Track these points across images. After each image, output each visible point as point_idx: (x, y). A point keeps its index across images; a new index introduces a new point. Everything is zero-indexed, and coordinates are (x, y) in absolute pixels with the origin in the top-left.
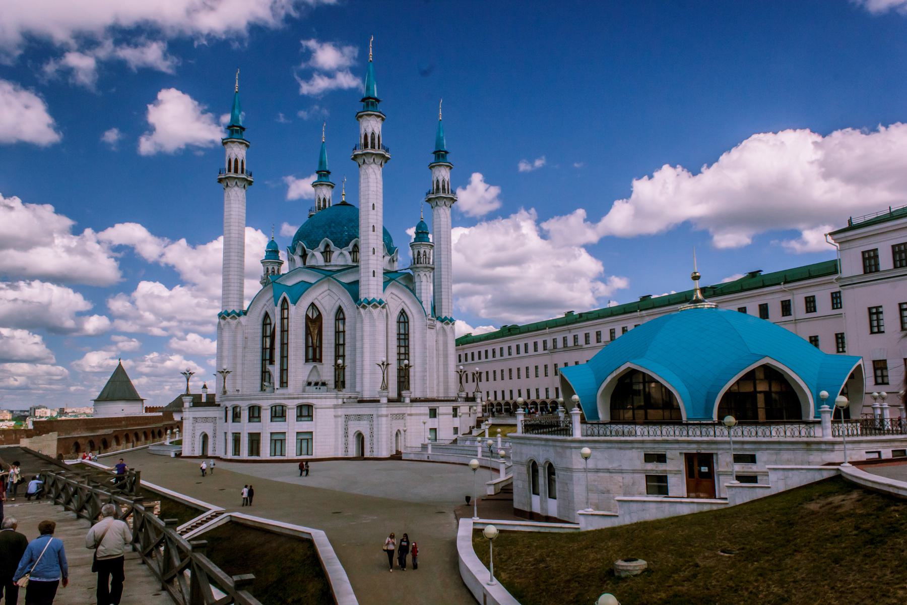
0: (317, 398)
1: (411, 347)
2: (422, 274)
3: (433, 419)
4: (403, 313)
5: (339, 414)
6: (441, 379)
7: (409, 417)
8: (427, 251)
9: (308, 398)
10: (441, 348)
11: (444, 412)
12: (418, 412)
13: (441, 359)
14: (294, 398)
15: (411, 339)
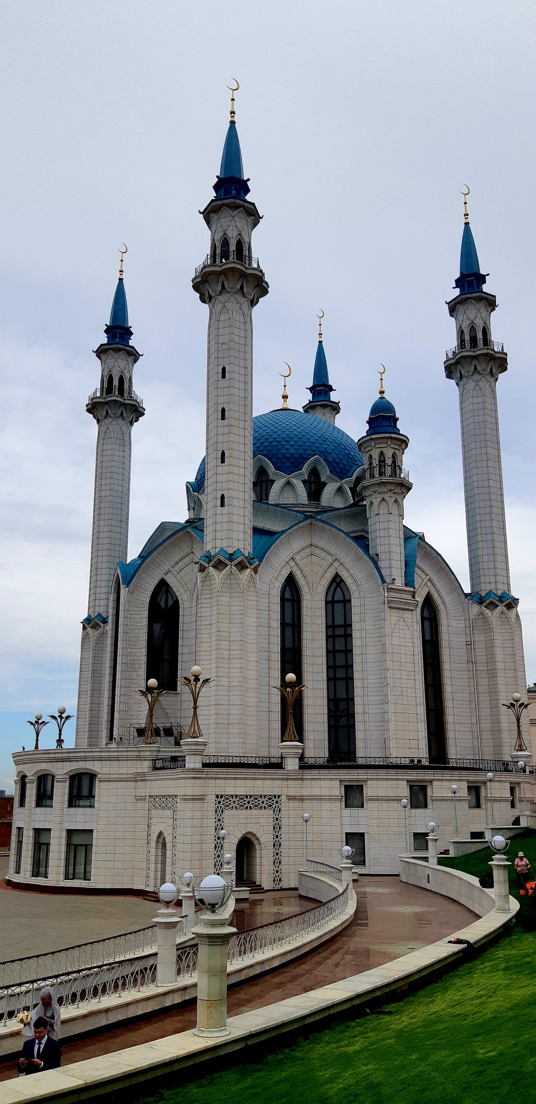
0: (101, 759)
1: (356, 651)
2: (376, 499)
3: (354, 811)
4: (337, 582)
5: (141, 792)
6: (486, 725)
7: (292, 804)
8: (384, 450)
9: (85, 759)
10: (481, 657)
11: (382, 793)
12: (317, 792)
13: (484, 682)
14: (63, 760)
15: (356, 634)
